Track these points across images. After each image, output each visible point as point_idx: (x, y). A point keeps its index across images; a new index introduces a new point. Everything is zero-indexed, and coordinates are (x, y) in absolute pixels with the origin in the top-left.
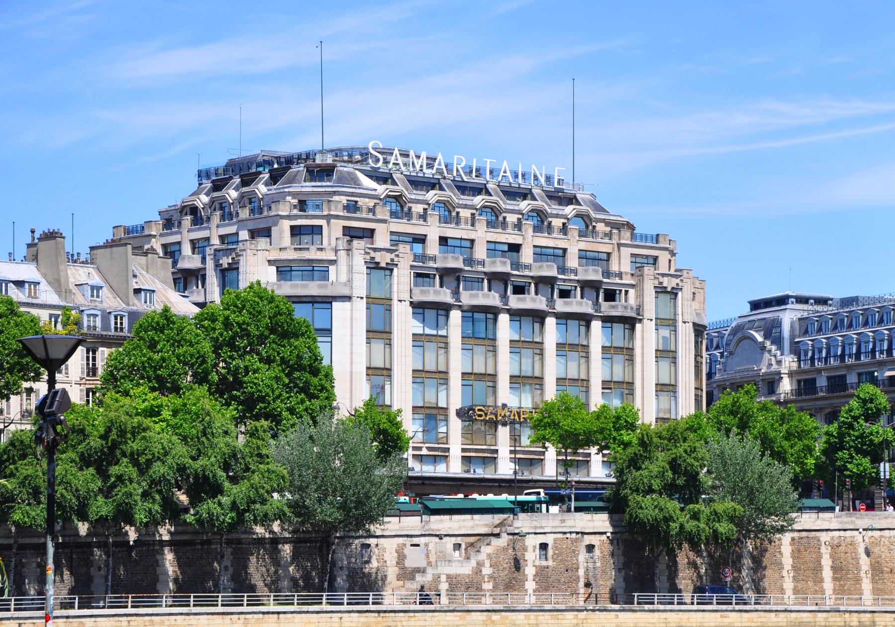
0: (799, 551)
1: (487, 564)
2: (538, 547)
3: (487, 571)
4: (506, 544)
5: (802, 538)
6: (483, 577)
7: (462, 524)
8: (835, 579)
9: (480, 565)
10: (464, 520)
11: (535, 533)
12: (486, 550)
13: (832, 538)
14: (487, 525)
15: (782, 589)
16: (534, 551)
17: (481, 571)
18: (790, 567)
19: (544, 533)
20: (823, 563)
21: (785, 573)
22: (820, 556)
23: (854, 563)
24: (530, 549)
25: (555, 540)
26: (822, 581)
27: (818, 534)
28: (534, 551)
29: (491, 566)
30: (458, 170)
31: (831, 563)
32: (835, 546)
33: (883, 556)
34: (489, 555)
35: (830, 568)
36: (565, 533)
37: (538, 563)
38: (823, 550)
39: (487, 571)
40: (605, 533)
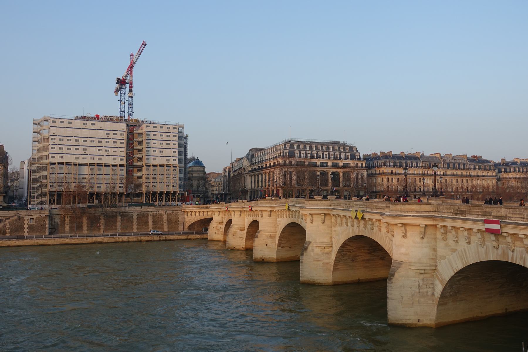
0: (140, 217)
1: (8, 224)
2: (29, 219)
3: (8, 226)
4: (16, 219)
5: (141, 214)
6: (7, 228)
7: (4, 213)
8: (153, 225)
9: (5, 225)
10: (5, 212)
11: (28, 216)
12: (7, 221)
13: (153, 214)
14: (14, 214)
15: (132, 228)
16: (28, 221)
17: (5, 227)
18: (136, 222)
19: (32, 216)
20: (149, 220)
21: (134, 224)
22: (148, 218)
23: (161, 220)
24: (26, 220)
25: (36, 217)
26: (148, 225)
27: (147, 213)
28: (28, 221)
29: (10, 225)
30: (114, 120)
31: (152, 220)
32: (154, 216)
33: (173, 218)
34: (9, 222)
35: (151, 222)
36: (41, 215)
37: (29, 224)
38: (149, 217)
39: (8, 226)
40: (62, 214)
